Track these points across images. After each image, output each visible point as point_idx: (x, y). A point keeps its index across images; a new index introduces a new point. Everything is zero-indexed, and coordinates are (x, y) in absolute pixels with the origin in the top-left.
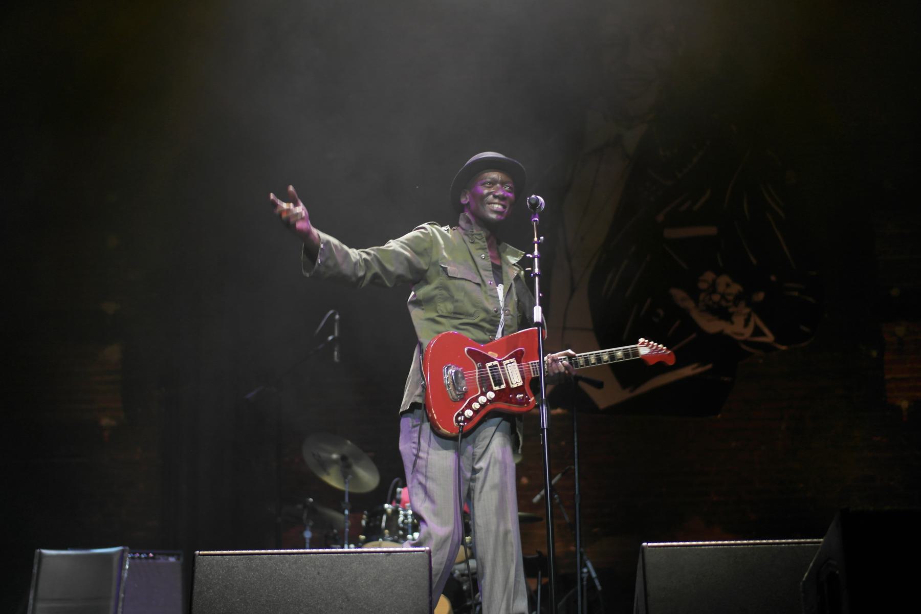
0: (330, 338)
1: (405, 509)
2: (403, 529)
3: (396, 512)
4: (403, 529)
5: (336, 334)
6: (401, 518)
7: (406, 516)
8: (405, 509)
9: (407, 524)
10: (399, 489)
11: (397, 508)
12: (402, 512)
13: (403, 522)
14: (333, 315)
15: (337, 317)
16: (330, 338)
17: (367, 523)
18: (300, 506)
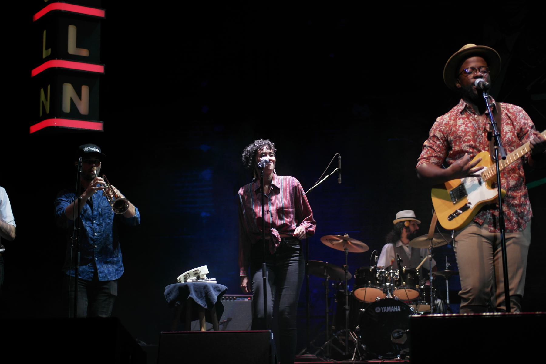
2: (378, 280)
4: (378, 280)
5: (340, 167)
6: (378, 274)
10: (376, 257)
13: (379, 276)
14: (338, 156)
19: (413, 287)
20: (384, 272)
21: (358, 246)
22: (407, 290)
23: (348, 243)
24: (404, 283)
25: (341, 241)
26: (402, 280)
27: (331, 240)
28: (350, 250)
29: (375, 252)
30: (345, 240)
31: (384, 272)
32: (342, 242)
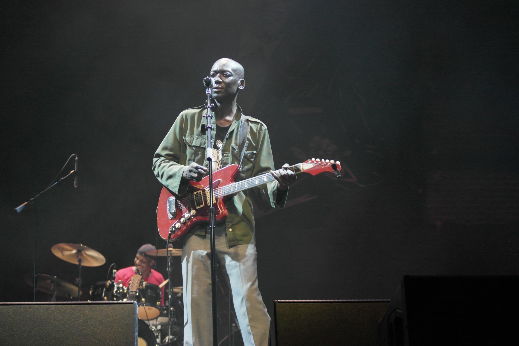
0: (72, 172)
1: (119, 283)
2: (116, 297)
3: (112, 286)
4: (116, 297)
7: (118, 288)
8: (119, 283)
9: (120, 292)
10: (114, 271)
11: (113, 283)
12: (116, 286)
13: (116, 291)
14: (74, 157)
15: (77, 158)
16: (72, 172)
17: (92, 293)
18: (49, 281)
19: (154, 305)
20: (122, 288)
21: (94, 258)
22: (147, 308)
23: (82, 255)
24: (143, 300)
25: (74, 251)
26: (141, 296)
27: (62, 250)
28: (84, 264)
29: (114, 265)
30: (79, 251)
31: (122, 288)
32: (76, 253)
